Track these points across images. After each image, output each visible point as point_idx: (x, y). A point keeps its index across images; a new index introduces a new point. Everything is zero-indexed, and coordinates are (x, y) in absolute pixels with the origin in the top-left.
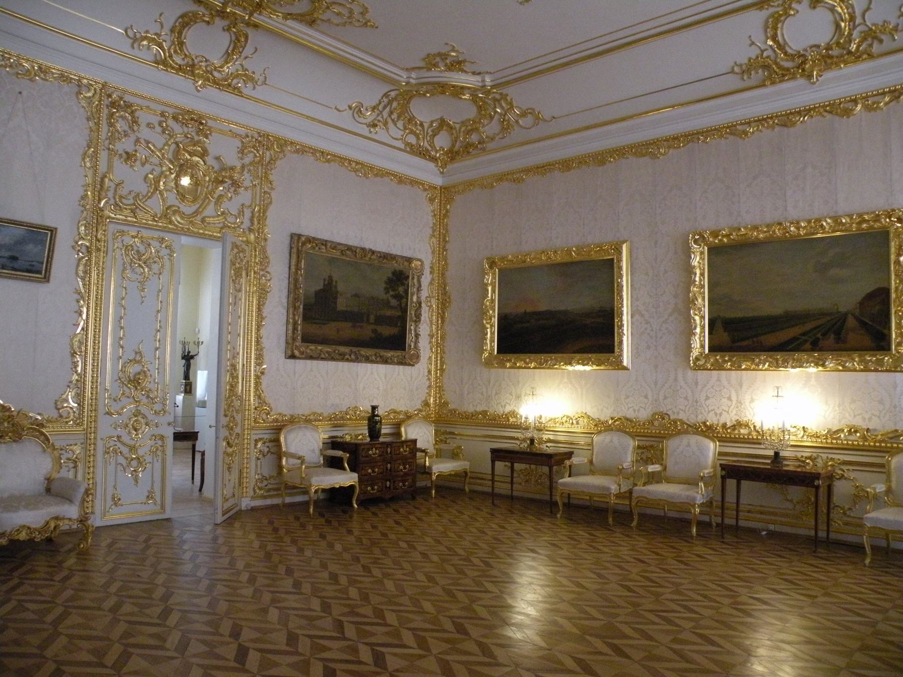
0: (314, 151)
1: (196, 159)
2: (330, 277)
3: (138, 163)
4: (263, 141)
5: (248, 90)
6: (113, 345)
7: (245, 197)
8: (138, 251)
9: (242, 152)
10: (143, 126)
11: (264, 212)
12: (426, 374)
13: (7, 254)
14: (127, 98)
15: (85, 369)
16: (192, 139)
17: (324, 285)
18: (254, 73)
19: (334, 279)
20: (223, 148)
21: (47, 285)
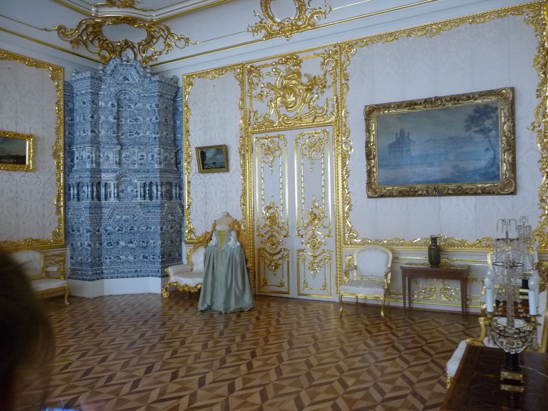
0: (380, 37)
1: (294, 82)
2: (402, 132)
3: (264, 97)
4: (340, 49)
5: (323, 21)
6: (259, 199)
7: (329, 93)
8: (268, 146)
9: (323, 64)
10: (265, 76)
11: (342, 99)
12: (539, 202)
13: (211, 162)
14: (256, 64)
15: (246, 213)
16: (291, 70)
17: (397, 138)
18: (320, 8)
19: (406, 131)
20: (311, 68)
21: (226, 173)
